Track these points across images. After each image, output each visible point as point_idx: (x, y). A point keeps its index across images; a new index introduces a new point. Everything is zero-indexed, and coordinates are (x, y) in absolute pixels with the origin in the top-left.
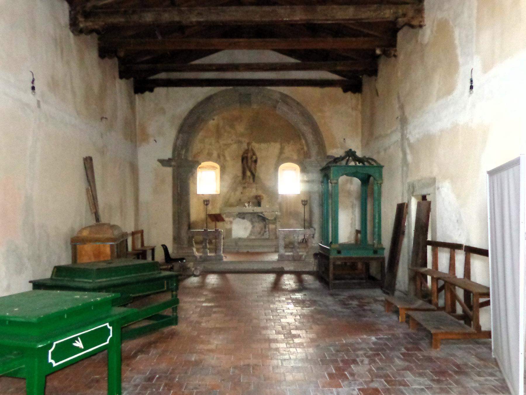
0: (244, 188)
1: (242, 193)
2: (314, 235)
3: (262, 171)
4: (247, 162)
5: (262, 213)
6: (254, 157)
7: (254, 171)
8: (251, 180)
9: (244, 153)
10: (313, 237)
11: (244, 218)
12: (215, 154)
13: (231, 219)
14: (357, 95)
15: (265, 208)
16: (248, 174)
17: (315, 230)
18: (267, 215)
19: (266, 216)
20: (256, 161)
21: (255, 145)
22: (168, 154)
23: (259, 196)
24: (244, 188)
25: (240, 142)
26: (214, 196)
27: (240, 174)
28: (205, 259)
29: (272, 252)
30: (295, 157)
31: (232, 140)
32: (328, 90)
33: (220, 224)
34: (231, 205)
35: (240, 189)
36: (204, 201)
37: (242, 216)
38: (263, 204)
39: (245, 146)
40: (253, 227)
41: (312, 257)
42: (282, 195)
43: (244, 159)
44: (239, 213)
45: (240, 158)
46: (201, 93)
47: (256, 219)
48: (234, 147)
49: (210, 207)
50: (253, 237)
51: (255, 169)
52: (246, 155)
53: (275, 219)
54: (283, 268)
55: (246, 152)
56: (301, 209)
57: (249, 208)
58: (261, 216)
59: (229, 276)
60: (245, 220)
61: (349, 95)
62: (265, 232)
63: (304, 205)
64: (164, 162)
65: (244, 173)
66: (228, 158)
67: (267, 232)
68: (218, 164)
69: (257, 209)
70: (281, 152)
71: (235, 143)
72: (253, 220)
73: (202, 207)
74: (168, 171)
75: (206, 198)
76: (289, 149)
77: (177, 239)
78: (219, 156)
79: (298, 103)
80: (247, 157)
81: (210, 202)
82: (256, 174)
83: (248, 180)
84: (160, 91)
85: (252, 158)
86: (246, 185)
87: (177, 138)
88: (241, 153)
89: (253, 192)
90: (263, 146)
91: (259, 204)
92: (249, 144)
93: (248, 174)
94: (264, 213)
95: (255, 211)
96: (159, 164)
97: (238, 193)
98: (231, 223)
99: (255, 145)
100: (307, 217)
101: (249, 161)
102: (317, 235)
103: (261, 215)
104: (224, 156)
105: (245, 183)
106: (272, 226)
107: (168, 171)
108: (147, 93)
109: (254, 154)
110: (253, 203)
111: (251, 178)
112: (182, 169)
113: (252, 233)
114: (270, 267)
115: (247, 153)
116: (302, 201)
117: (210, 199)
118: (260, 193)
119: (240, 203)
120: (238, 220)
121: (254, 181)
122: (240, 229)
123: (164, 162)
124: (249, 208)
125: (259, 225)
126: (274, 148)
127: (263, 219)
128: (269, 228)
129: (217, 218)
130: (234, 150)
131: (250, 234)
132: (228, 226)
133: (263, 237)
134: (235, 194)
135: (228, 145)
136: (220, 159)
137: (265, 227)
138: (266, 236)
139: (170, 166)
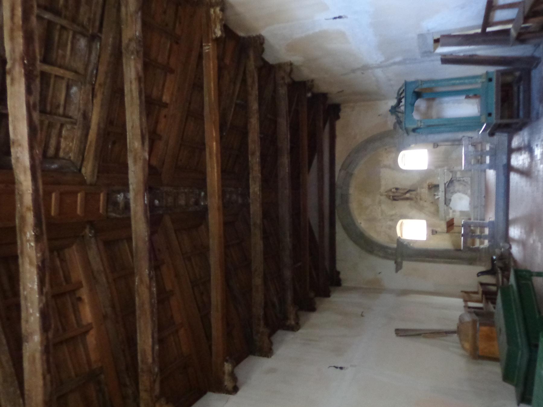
0: (421, 199)
2: (469, 137)
3: (406, 184)
4: (398, 196)
5: (445, 184)
6: (393, 190)
7: (406, 191)
8: (414, 193)
9: (389, 199)
10: (472, 138)
11: (450, 200)
12: (390, 223)
13: (451, 211)
14: (342, 107)
15: (442, 180)
16: (408, 195)
17: (464, 136)
18: (447, 179)
19: (450, 179)
20: (397, 189)
21: (383, 189)
22: (391, 264)
23: (429, 186)
24: (421, 199)
25: (380, 203)
26: (429, 226)
27: (408, 203)
28: (492, 237)
29: (485, 175)
30: (394, 155)
32: (338, 132)
33: (456, 222)
34: (437, 211)
35: (422, 203)
36: (433, 234)
37: (447, 202)
38: (436, 183)
39: (383, 198)
40: (459, 191)
41: (492, 138)
42: (429, 165)
43: (395, 199)
44: (445, 204)
45: (395, 202)
46: (340, 234)
47: (451, 189)
48: (384, 207)
49: (439, 229)
50: (469, 191)
51: (404, 189)
53: (452, 172)
54: (504, 166)
55: (388, 197)
56: (442, 148)
57: (441, 194)
58: (449, 184)
59: (511, 217)
60: (453, 199)
61: (342, 114)
62: (464, 181)
63: (438, 146)
64: (399, 267)
65: (407, 199)
66: (393, 212)
67: (464, 178)
68: (398, 221)
69: (442, 188)
70: (389, 167)
71: (380, 206)
72: (452, 191)
73: (437, 236)
74: (406, 264)
75: (430, 233)
76: (386, 160)
77: (471, 261)
78: (392, 220)
79: (349, 156)
80: (393, 196)
81: (434, 229)
82: (409, 188)
84: (339, 266)
85: (394, 192)
86: (419, 198)
87: (377, 255)
88: (390, 201)
89: (424, 191)
90: (383, 182)
91: (436, 187)
92: (381, 195)
93: (408, 195)
94: (446, 182)
95: (444, 190)
96: (399, 272)
97: (425, 204)
98: (454, 211)
99: (383, 189)
100: (449, 143)
101: (396, 194)
102: (470, 134)
103: (447, 184)
104: (392, 216)
106: (459, 175)
107: (406, 264)
108: (342, 276)
109: (391, 190)
110: (435, 191)
111: (411, 192)
112: (403, 253)
113: (465, 193)
114: (502, 178)
115: (390, 196)
116: (434, 147)
117: (431, 229)
118: (426, 185)
119: (435, 203)
120: (451, 205)
122: (461, 203)
123: (399, 267)
124: (441, 194)
125: (457, 186)
126: (385, 173)
127: (451, 182)
128: (459, 178)
129: (450, 225)
130: (387, 208)
131: (466, 194)
132: (458, 214)
133: (469, 182)
135: (382, 212)
136: (395, 219)
137: (459, 181)
138: (468, 179)
139: (401, 263)
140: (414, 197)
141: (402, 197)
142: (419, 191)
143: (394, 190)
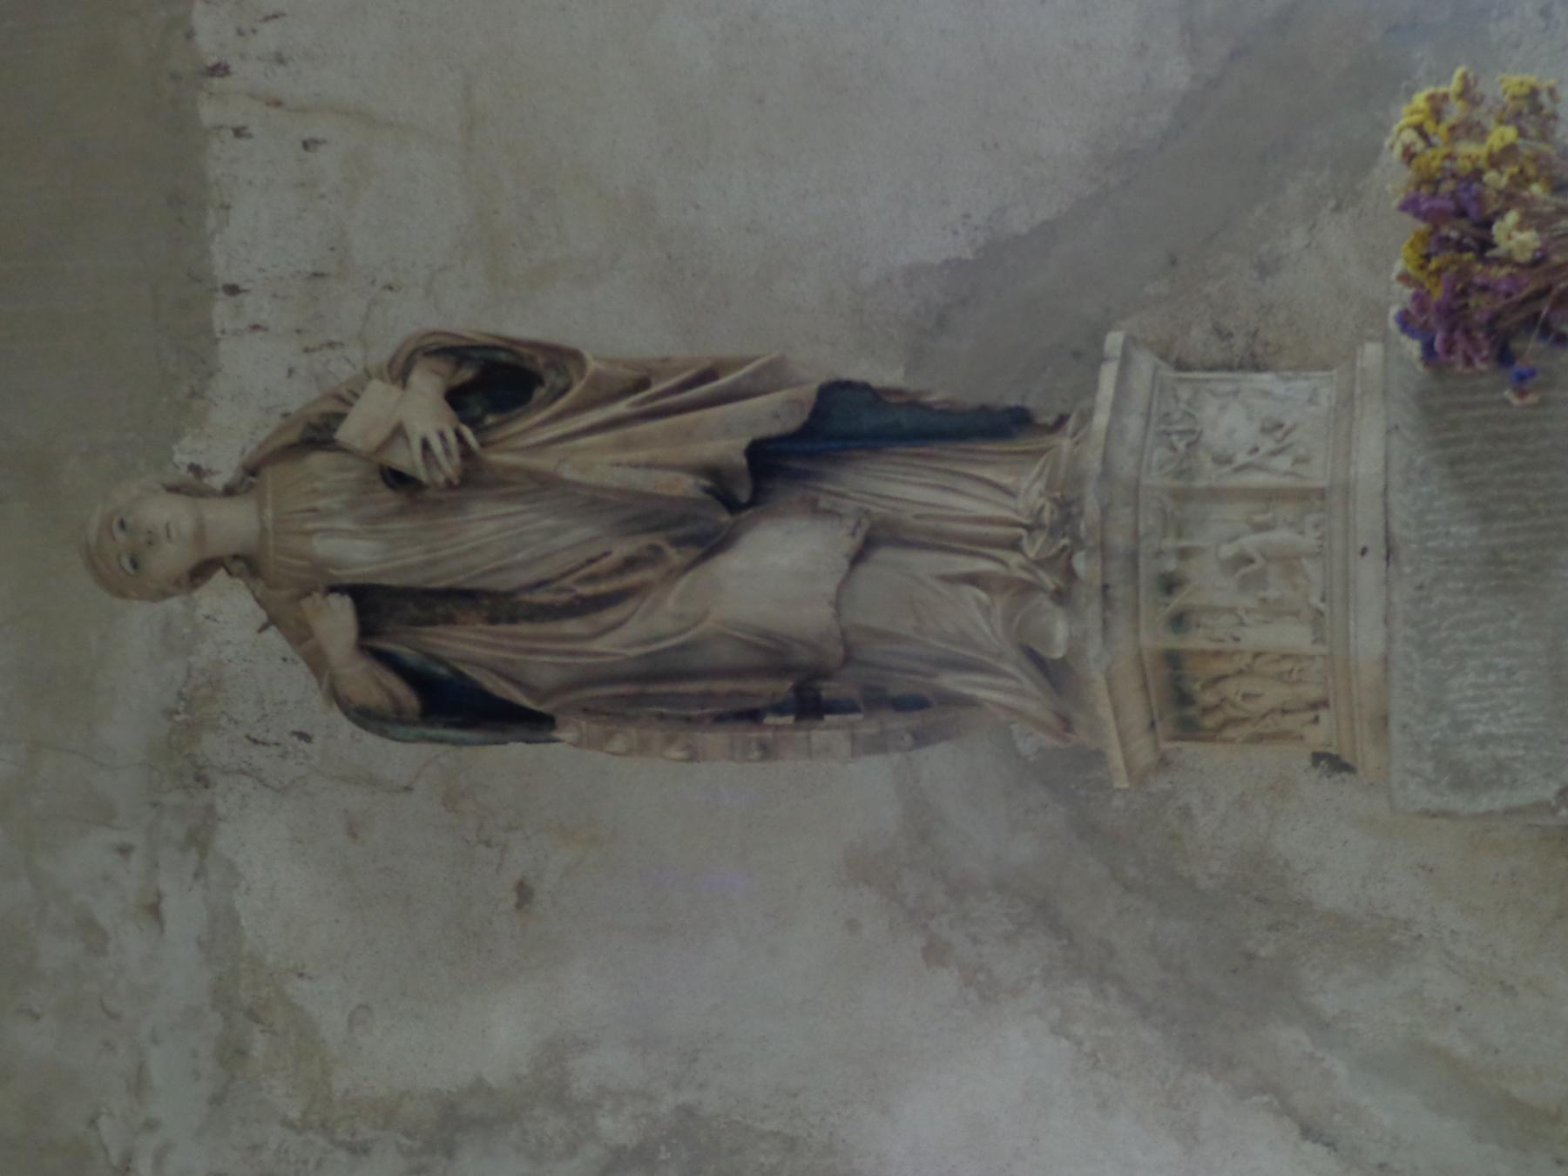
0: (1184, 700)
1: (1333, 763)
4: (494, 605)
7: (723, 436)
16: (779, 572)
20: (494, 381)
24: (1184, 700)
25: (184, 761)
31: (154, 910)
48: (272, 864)
51: (705, 385)
52: (337, 622)
65: (797, 689)
66: (497, 1036)
71: (199, 840)
83: (934, 609)
90: (256, 232)
92: (124, 569)
97: (1335, 849)
101: (487, 540)
105: (1055, 674)
109: (318, 435)
111: (904, 487)
118: (1359, 262)
121: (1004, 425)
134: (1377, 943)
140: (974, 618)
141: (620, 639)
142: (1116, 412)
143: (422, 412)
